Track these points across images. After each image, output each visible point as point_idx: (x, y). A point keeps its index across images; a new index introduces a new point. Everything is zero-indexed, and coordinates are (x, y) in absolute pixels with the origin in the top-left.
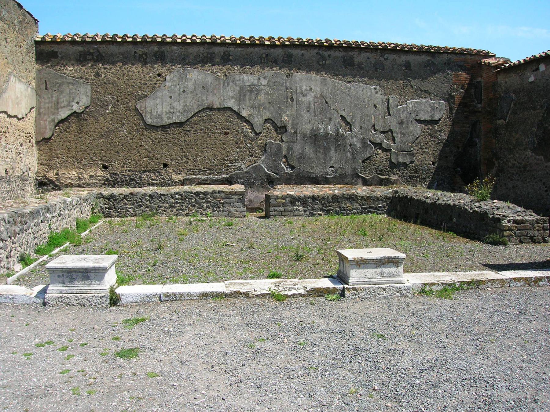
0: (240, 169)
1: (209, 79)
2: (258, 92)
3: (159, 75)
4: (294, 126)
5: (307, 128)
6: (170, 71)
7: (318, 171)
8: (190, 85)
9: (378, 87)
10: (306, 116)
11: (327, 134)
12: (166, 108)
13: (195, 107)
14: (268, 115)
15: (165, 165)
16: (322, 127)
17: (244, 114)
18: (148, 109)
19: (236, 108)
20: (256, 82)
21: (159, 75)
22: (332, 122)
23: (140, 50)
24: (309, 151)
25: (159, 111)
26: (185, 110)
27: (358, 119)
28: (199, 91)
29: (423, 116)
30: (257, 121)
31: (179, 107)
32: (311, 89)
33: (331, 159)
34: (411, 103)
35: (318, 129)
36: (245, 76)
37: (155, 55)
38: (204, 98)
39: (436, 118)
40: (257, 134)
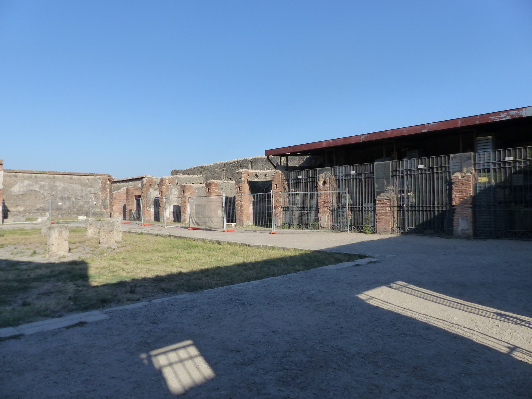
1: (31, 183)
2: (46, 186)
6: (19, 180)
8: (25, 184)
10: (59, 193)
11: (65, 197)
12: (18, 190)
14: (48, 192)
15: (17, 206)
18: (12, 191)
19: (39, 191)
23: (9, 174)
26: (23, 192)
29: (92, 192)
30: (45, 194)
31: (22, 190)
34: (89, 189)
40: (45, 197)
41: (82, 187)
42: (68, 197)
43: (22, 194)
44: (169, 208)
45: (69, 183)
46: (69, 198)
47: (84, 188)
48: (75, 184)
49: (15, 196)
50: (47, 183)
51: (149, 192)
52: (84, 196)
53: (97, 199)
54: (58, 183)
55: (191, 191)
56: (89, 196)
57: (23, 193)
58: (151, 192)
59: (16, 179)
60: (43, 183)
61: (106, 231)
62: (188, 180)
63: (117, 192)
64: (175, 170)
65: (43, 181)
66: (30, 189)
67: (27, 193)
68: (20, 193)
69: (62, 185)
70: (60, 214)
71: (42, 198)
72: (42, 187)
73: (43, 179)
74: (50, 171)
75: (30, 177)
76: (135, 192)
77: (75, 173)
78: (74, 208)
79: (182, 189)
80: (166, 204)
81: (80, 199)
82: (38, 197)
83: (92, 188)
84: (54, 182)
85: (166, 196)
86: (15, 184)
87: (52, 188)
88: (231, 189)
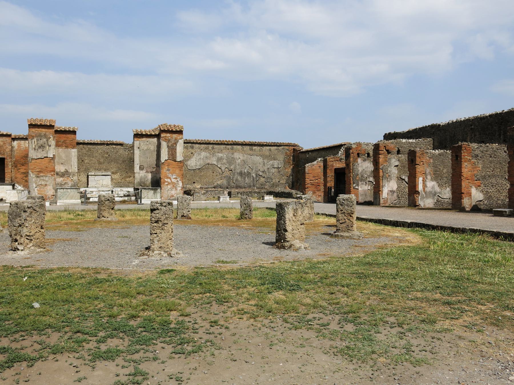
0: (218, 184)
1: (208, 155)
2: (223, 159)
3: (192, 153)
4: (235, 170)
5: (239, 171)
7: (242, 184)
8: (202, 157)
9: (261, 157)
10: (238, 167)
11: (245, 172)
12: (194, 164)
13: (204, 164)
14: (227, 167)
15: (194, 183)
16: (243, 170)
17: (219, 166)
18: (189, 164)
20: (222, 156)
21: (192, 153)
22: (246, 169)
24: (239, 178)
25: (192, 165)
27: (254, 168)
28: (205, 158)
29: (276, 166)
30: (223, 168)
31: (198, 164)
32: (240, 158)
33: (246, 181)
34: (271, 162)
35: (242, 171)
36: (219, 154)
37: (191, 147)
38: (206, 161)
39: (280, 167)
41: (263, 159)
42: (248, 172)
43: (199, 169)
44: (386, 185)
45: (249, 155)
46: (249, 174)
47: (266, 161)
48: (255, 156)
49: (192, 171)
50: (225, 154)
51: (357, 164)
52: (266, 171)
53: (281, 174)
54: (237, 155)
55: (424, 161)
56: (271, 171)
57: (200, 167)
58: (359, 163)
59: (193, 151)
60: (220, 155)
61: (346, 212)
62: (413, 145)
63: (310, 165)
64: (390, 133)
65: (221, 153)
66: (207, 163)
67: (203, 167)
68: (197, 168)
69: (242, 158)
70: (239, 193)
71: (220, 174)
72: (219, 159)
73: (221, 151)
74: (228, 140)
75: (206, 148)
76: (335, 164)
77: (256, 142)
78: (254, 186)
79: (410, 158)
80: (384, 180)
81: (261, 175)
82: (215, 172)
83: (275, 161)
84: (233, 154)
85: (383, 168)
86: (192, 156)
87: (231, 161)
88: (491, 157)
